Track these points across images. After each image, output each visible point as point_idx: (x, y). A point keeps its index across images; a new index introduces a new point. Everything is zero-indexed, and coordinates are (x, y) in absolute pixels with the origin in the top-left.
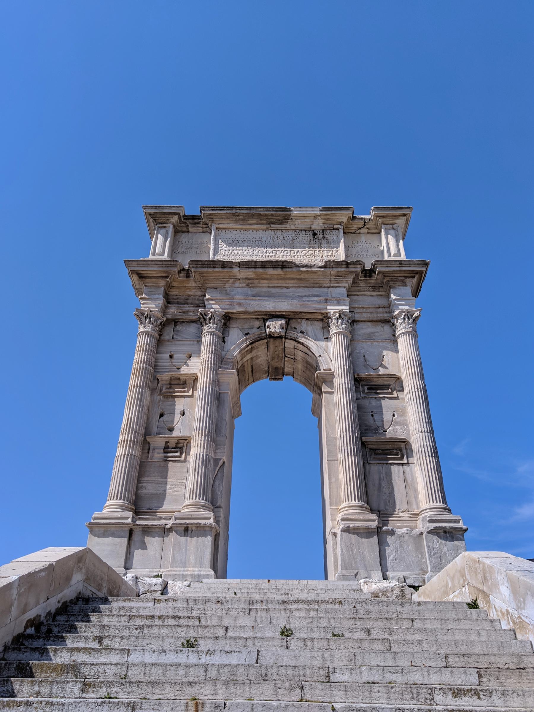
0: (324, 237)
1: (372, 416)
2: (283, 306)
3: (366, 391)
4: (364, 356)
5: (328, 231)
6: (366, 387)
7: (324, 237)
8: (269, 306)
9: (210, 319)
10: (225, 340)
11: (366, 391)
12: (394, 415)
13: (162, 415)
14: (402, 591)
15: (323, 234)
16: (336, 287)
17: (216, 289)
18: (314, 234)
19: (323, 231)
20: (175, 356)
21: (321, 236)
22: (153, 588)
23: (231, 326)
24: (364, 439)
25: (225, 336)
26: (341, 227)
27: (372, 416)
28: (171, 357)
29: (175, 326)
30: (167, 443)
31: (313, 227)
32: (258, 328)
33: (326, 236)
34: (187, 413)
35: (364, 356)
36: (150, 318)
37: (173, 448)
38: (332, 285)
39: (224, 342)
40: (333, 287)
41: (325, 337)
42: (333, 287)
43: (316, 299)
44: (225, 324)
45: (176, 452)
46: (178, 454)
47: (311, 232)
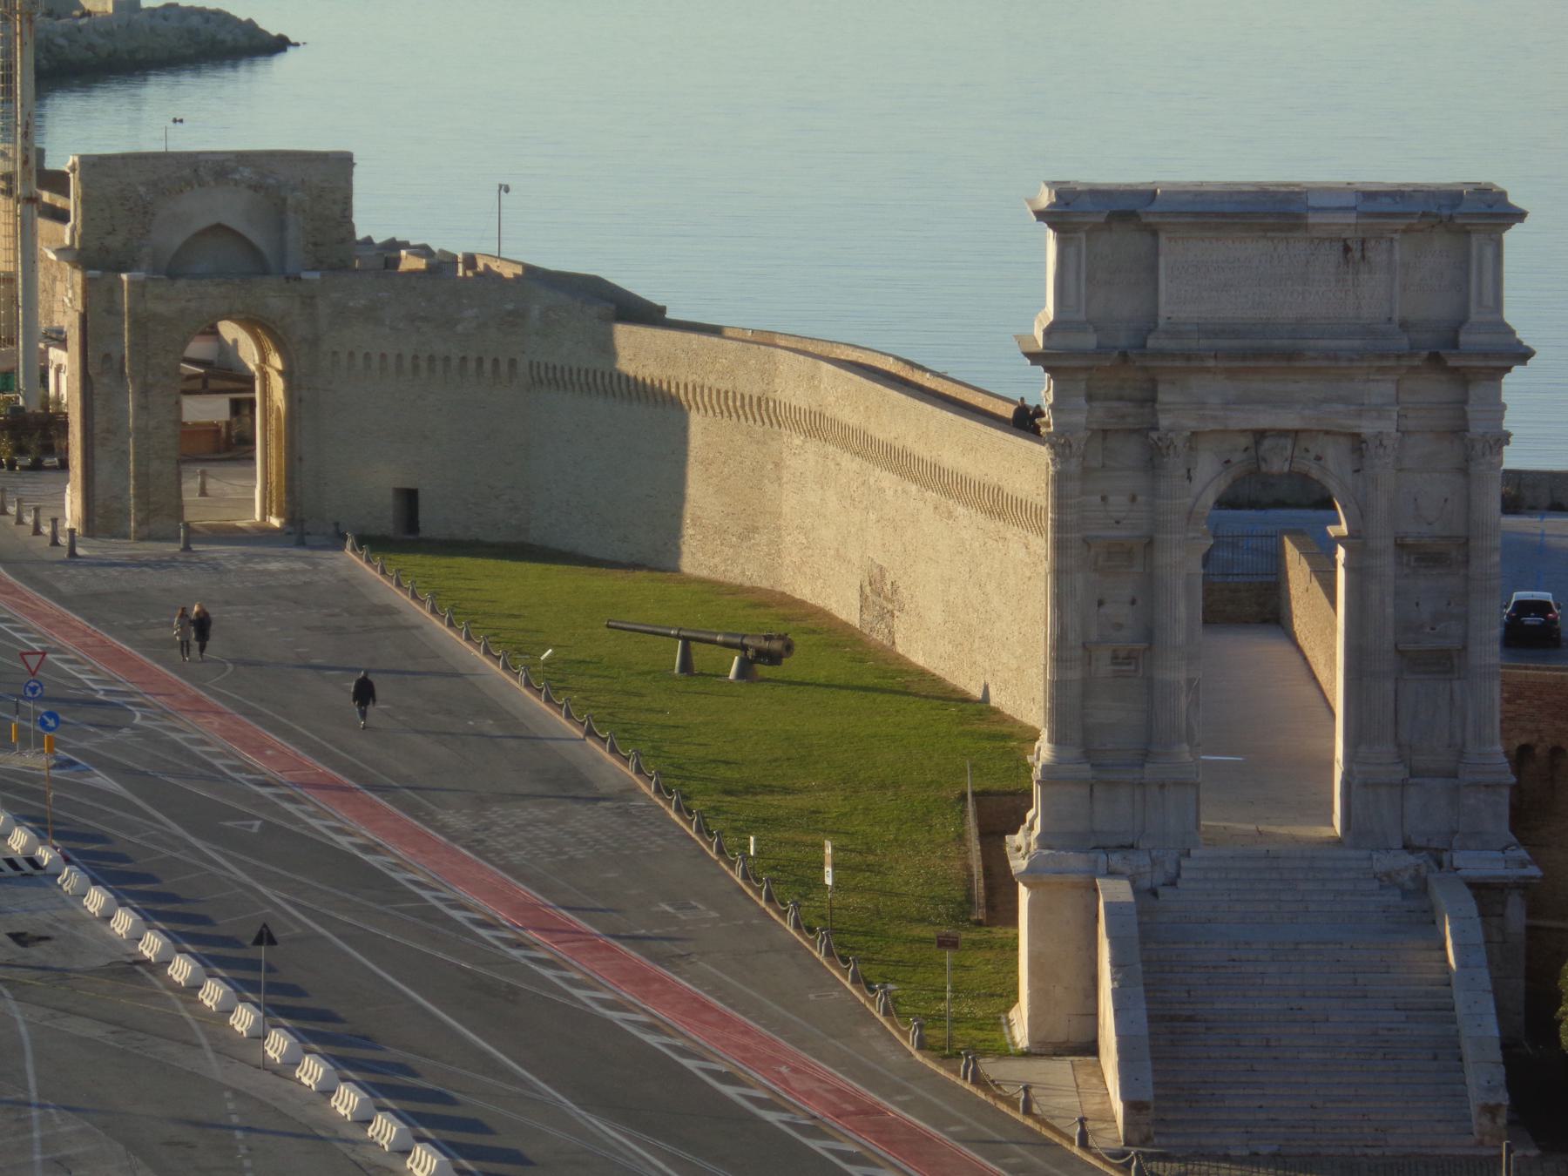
0: (1363, 257)
1: (1417, 604)
2: (1288, 419)
3: (1412, 564)
4: (1416, 500)
5: (1373, 243)
6: (1412, 558)
7: (1363, 257)
8: (1265, 419)
9: (1168, 448)
11: (1412, 564)
12: (1449, 604)
13: (1100, 603)
14: (1416, 870)
15: (1363, 250)
16: (1378, 381)
17: (1174, 383)
18: (1347, 249)
19: (1363, 242)
20: (1111, 499)
21: (1358, 255)
22: (1142, 870)
24: (1401, 647)
27: (1417, 604)
28: (1104, 499)
29: (1104, 439)
30: (1114, 651)
31: (1344, 236)
32: (1246, 449)
33: (1368, 254)
35: (1416, 500)
36: (1070, 446)
37: (1124, 659)
38: (1371, 377)
39: (1190, 478)
40: (1373, 380)
41: (1356, 468)
42: (1373, 380)
43: (1340, 407)
44: (1191, 448)
45: (1129, 664)
46: (1132, 667)
47: (1339, 246)
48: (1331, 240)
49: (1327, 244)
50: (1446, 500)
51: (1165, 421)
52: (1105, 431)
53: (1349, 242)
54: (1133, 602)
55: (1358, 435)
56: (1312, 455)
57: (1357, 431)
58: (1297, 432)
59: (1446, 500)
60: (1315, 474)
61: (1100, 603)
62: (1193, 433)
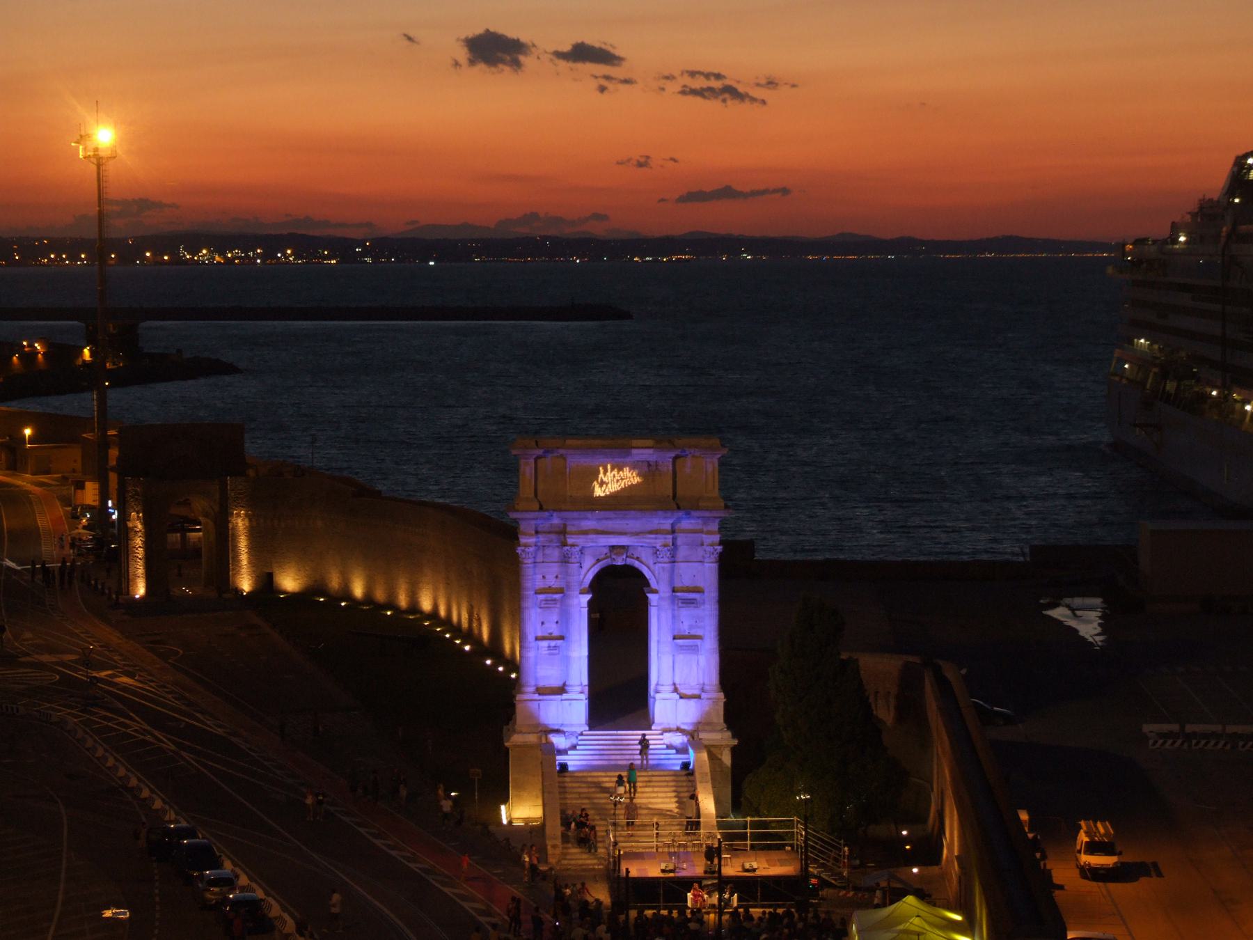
10: (582, 565)
11: (680, 604)
13: (543, 623)
18: (649, 465)
20: (547, 577)
23: (586, 553)
25: (582, 562)
26: (671, 460)
28: (544, 577)
29: (543, 550)
30: (549, 644)
34: (560, 622)
39: (581, 567)
44: (582, 553)
45: (556, 650)
46: (557, 651)
47: (646, 464)
48: (643, 462)
49: (640, 463)
50: (694, 576)
51: (570, 541)
52: (544, 546)
53: (651, 463)
54: (557, 622)
55: (655, 547)
56: (635, 556)
57: (654, 545)
58: (628, 546)
59: (694, 576)
60: (637, 564)
61: (543, 623)
62: (583, 547)
